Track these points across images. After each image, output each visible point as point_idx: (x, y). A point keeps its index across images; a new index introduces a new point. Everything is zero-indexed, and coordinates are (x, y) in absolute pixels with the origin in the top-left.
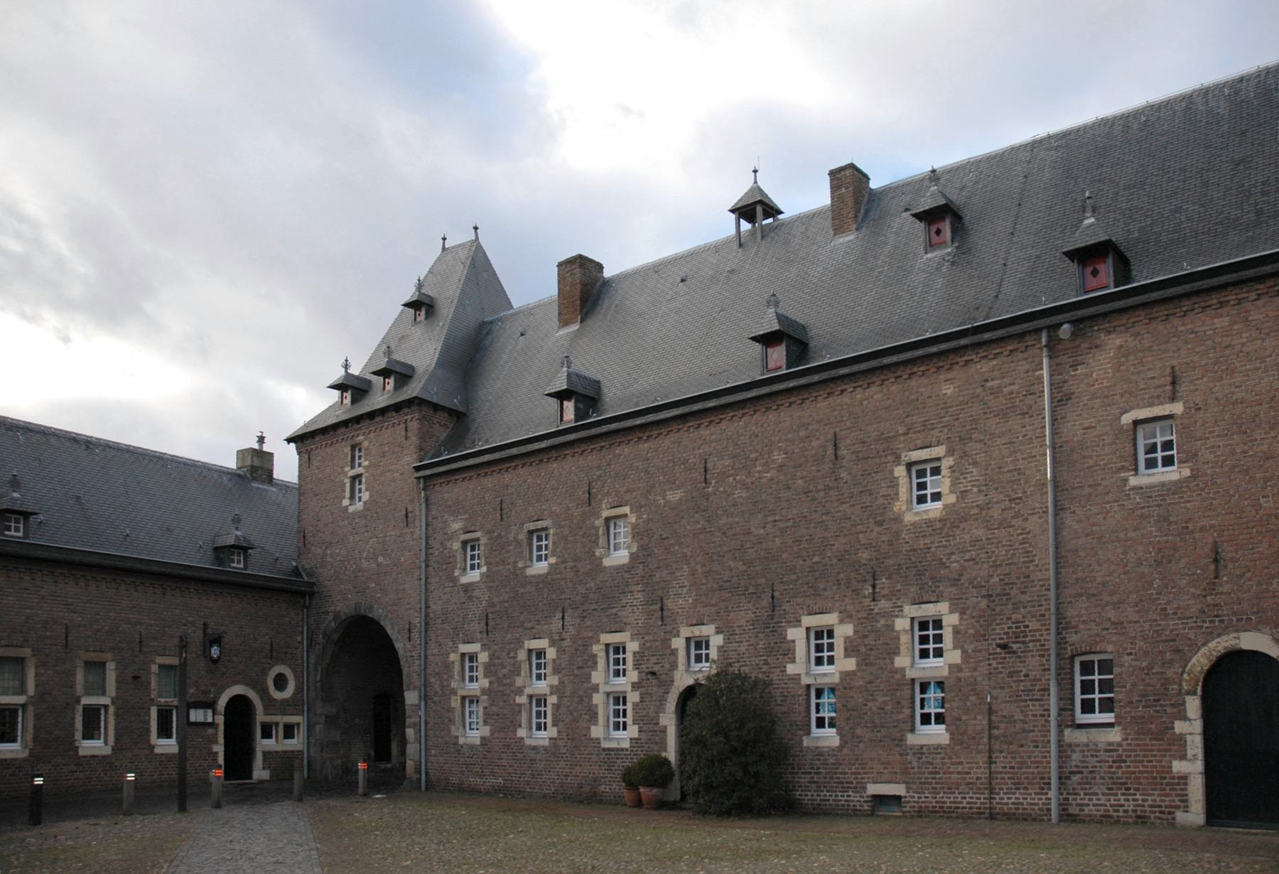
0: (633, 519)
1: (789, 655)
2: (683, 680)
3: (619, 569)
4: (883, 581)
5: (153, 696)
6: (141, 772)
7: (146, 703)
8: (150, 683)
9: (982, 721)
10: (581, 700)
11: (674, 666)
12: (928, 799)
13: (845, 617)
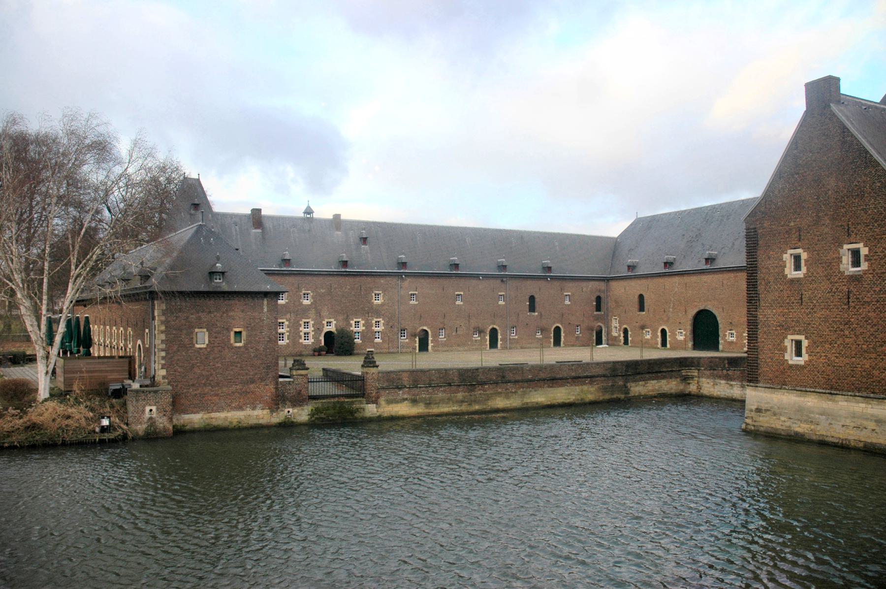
0: (312, 294)
1: (351, 326)
2: (327, 329)
3: (308, 305)
4: (370, 314)
9: (387, 338)
10: (296, 334)
11: (323, 327)
12: (378, 351)
13: (363, 320)
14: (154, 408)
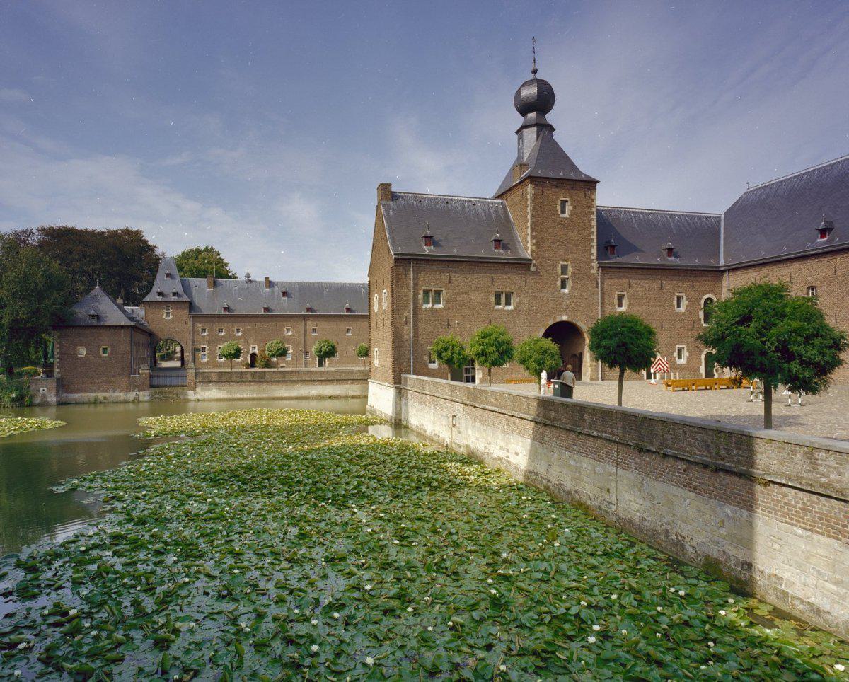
2: (251, 352)
14: (45, 389)
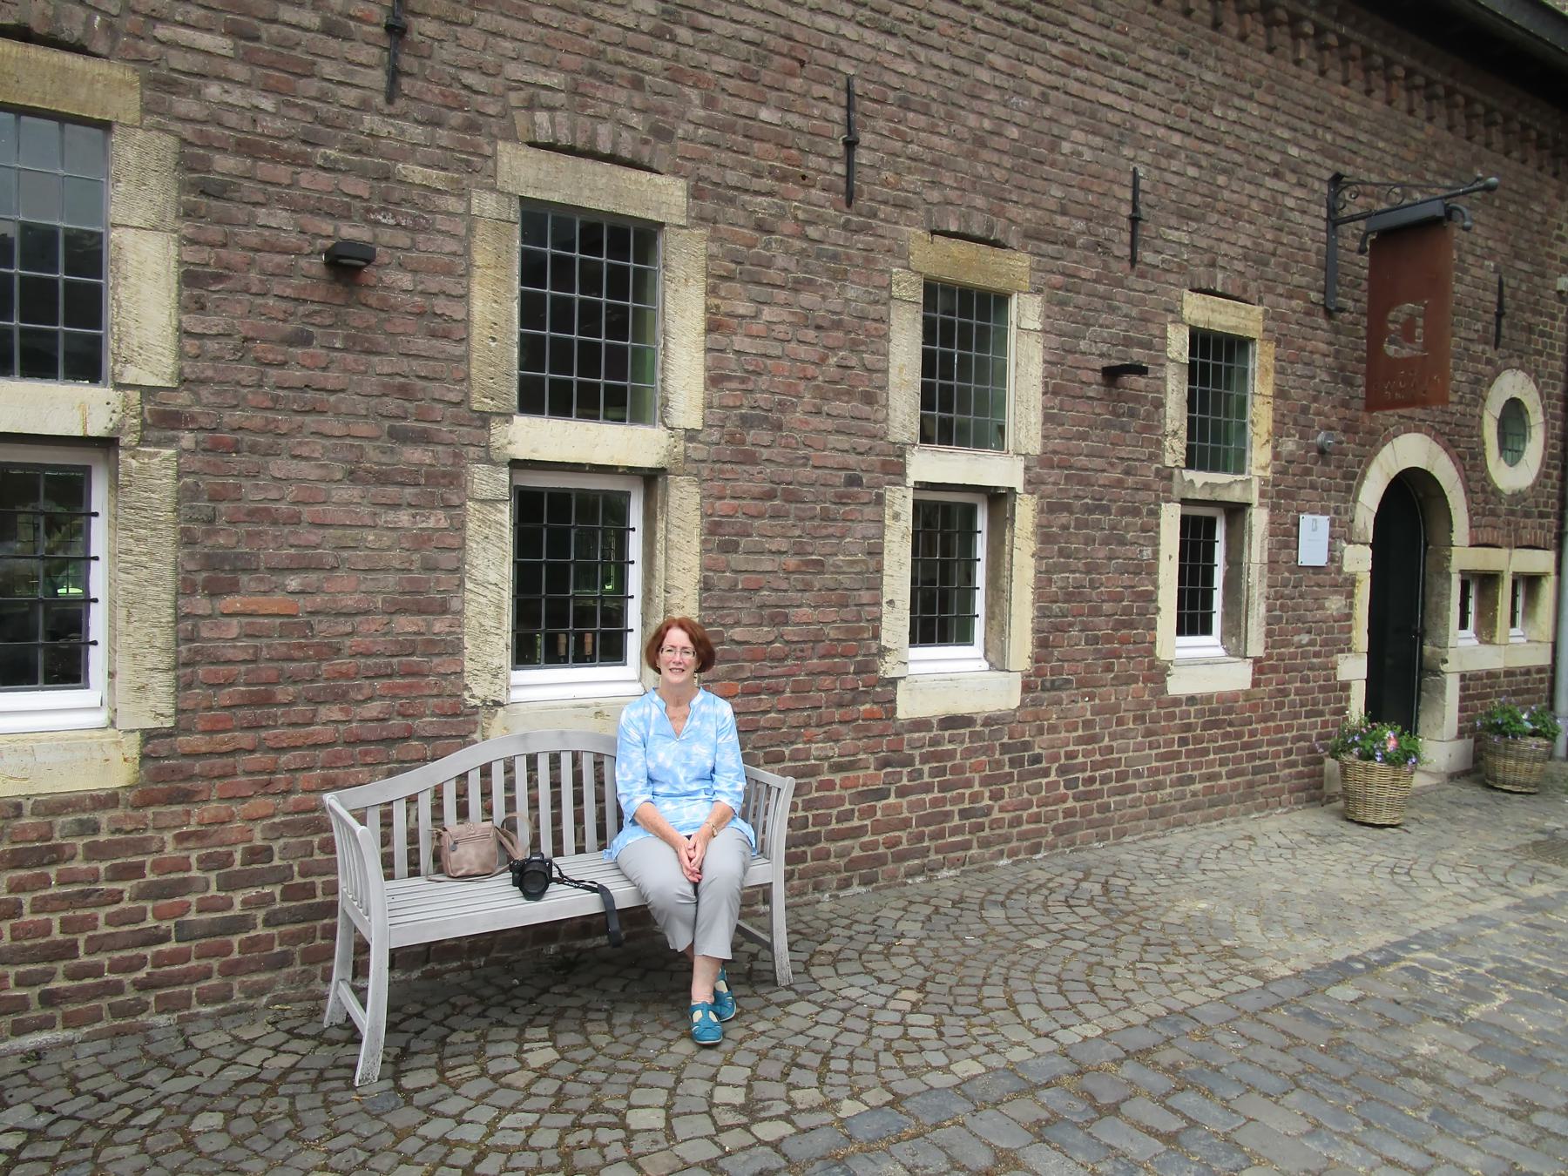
5: (1169, 463)
6: (1122, 776)
7: (1146, 487)
8: (1159, 404)
